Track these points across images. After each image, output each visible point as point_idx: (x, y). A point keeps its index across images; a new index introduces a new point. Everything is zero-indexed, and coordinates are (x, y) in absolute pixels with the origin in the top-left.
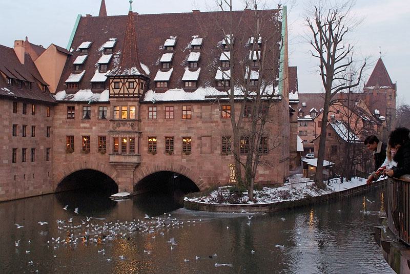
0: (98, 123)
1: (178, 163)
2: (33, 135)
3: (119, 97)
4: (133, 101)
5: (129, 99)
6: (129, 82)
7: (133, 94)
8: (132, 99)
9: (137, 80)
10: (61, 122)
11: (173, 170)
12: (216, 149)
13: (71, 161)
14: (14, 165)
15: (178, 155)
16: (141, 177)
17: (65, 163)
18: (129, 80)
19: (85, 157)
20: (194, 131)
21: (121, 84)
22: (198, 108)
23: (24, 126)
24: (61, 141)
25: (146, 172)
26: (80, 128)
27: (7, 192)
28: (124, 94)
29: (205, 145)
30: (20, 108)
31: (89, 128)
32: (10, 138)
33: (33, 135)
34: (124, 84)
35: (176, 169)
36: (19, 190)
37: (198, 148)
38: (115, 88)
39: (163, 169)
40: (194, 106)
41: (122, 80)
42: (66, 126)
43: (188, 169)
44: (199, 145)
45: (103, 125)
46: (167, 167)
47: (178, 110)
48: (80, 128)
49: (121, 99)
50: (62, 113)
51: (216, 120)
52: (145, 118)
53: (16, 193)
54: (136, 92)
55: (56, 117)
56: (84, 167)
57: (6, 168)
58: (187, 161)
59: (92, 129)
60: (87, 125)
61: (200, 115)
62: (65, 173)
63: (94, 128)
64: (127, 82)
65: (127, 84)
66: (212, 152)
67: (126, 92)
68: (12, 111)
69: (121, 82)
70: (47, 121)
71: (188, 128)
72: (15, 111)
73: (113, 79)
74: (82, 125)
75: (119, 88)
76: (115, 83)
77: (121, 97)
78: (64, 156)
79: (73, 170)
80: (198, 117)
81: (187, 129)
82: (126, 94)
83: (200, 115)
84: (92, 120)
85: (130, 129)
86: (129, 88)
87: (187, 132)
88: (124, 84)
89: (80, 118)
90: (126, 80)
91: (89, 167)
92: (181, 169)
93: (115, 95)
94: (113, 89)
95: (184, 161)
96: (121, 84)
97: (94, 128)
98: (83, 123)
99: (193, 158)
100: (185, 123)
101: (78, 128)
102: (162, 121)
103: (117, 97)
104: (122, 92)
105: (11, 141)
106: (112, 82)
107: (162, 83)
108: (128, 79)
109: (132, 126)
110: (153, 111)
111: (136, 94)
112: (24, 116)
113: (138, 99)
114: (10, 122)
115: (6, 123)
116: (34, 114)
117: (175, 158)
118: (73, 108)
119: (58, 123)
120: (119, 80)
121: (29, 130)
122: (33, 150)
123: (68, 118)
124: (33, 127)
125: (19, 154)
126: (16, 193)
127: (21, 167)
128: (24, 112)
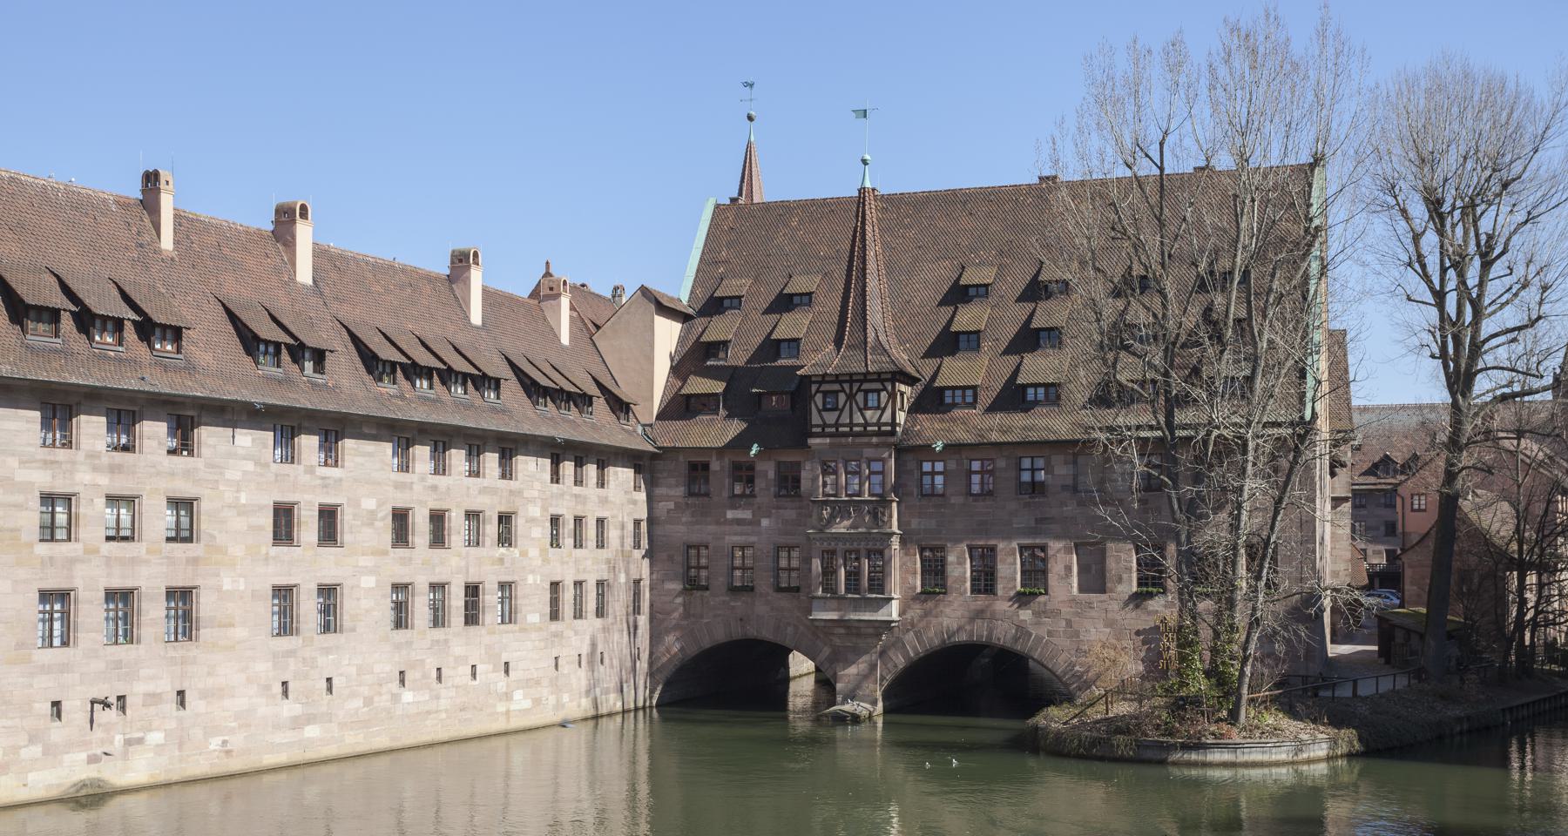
0: (778, 508)
2: (601, 544)
4: (877, 446)
5: (865, 440)
6: (866, 392)
7: (879, 424)
8: (874, 440)
10: (671, 505)
11: (994, 641)
14: (555, 626)
16: (901, 662)
18: (866, 386)
21: (842, 398)
22: (1066, 463)
23: (578, 520)
24: (671, 558)
25: (914, 648)
27: (537, 702)
28: (851, 425)
30: (568, 468)
32: (543, 551)
33: (601, 544)
34: (851, 397)
35: (1003, 634)
36: (566, 698)
38: (826, 409)
40: (1054, 458)
41: (846, 386)
43: (1039, 639)
45: (790, 514)
46: (979, 631)
49: (843, 440)
50: (672, 481)
53: (559, 706)
54: (887, 417)
56: (737, 633)
57: (534, 635)
59: (759, 523)
60: (746, 514)
61: (1069, 482)
63: (765, 522)
64: (859, 390)
67: (858, 419)
68: (548, 477)
69: (843, 390)
70: (635, 502)
71: (1039, 521)
72: (556, 477)
73: (821, 383)
74: (730, 514)
75: (835, 409)
76: (825, 394)
77: (845, 435)
78: (679, 600)
79: (707, 643)
80: (1065, 488)
81: (1032, 523)
83: (1069, 482)
84: (758, 500)
86: (867, 408)
87: (1033, 532)
88: (851, 397)
89: (725, 494)
91: (752, 632)
92: (1016, 639)
94: (819, 411)
95: (1026, 615)
96: (842, 398)
97: (765, 522)
98: (734, 507)
101: (718, 523)
102: (956, 500)
103: (831, 435)
105: (546, 561)
107: (958, 393)
108: (862, 382)
110: (933, 473)
111: (886, 424)
112: (577, 490)
113: (892, 440)
114: (544, 509)
115: (535, 511)
116: (601, 483)
118: (706, 466)
119: (663, 507)
120: (836, 387)
121: (591, 531)
122: (600, 584)
123: (691, 494)
124: (601, 522)
125: (568, 596)
126: (559, 706)
127: (571, 633)
128: (578, 481)
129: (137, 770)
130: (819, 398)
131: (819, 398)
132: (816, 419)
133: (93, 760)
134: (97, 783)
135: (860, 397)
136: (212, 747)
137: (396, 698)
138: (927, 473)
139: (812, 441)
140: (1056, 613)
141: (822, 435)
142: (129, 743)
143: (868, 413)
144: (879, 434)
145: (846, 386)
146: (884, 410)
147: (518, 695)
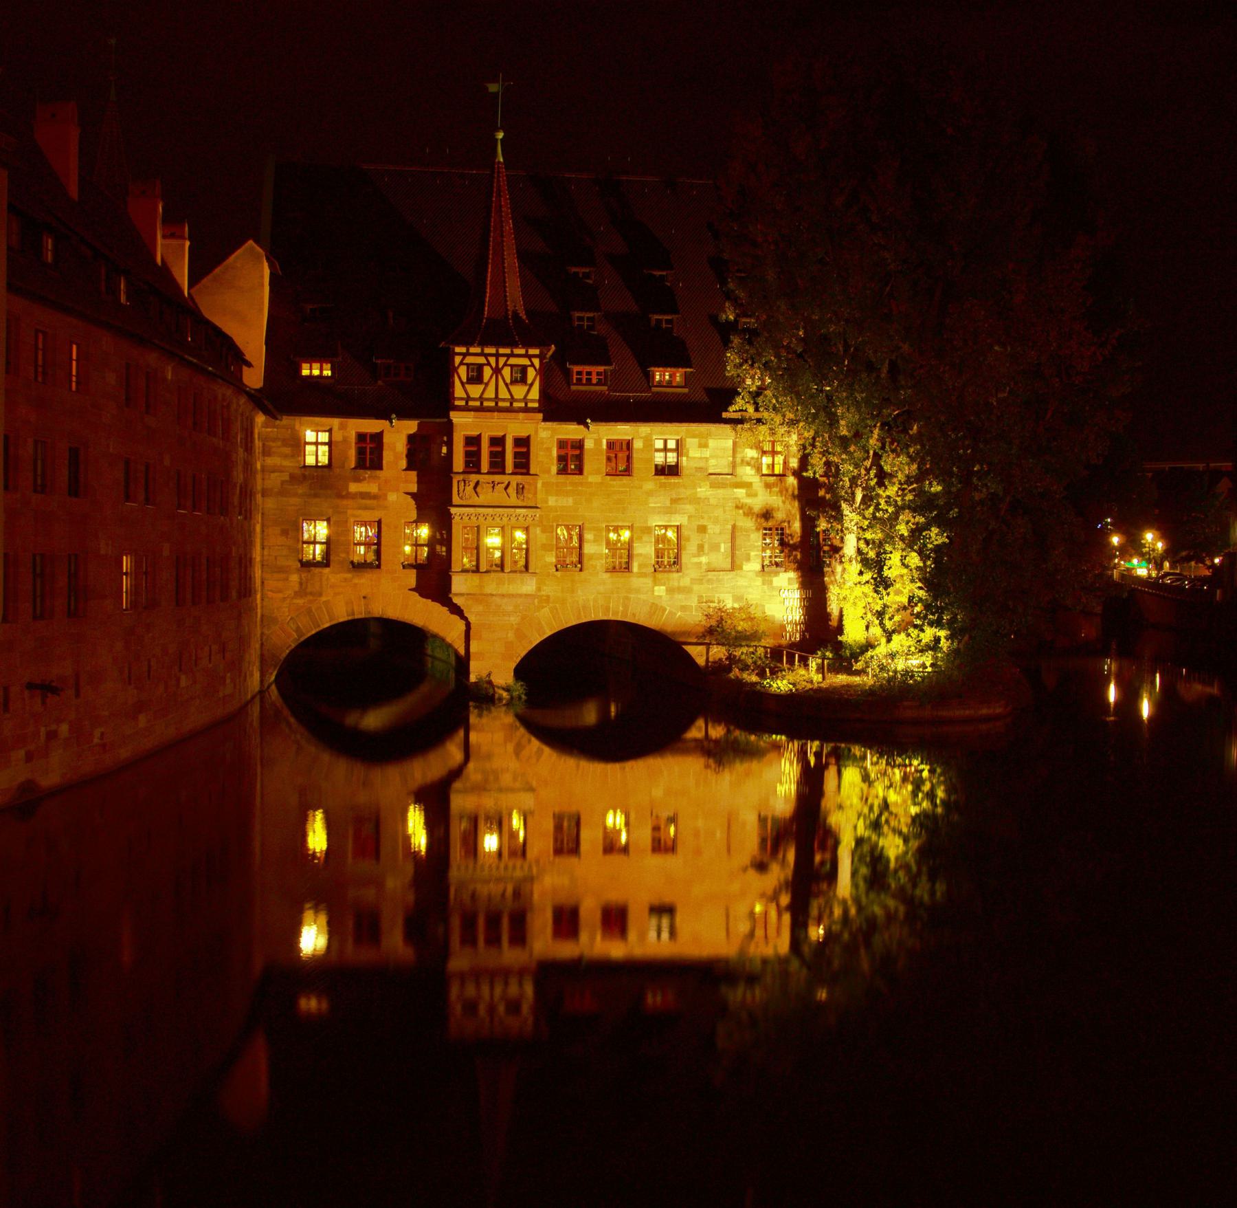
1: (642, 597)
3: (481, 409)
7: (525, 400)
8: (521, 415)
9: (536, 362)
10: (286, 477)
12: (748, 559)
13: (320, 595)
15: (644, 575)
16: (537, 639)
17: (300, 601)
18: (512, 361)
19: (363, 581)
20: (690, 508)
21: (487, 372)
26: (350, 496)
29: (715, 547)
31: (375, 497)
34: (497, 371)
37: (699, 556)
39: (601, 616)
41: (492, 360)
42: (301, 490)
44: (701, 548)
47: (642, 450)
48: (350, 496)
51: (746, 479)
52: (548, 471)
54: (535, 394)
55: (270, 461)
58: (670, 591)
62: (298, 630)
64: (505, 364)
65: (506, 372)
66: (734, 566)
67: (504, 393)
71: (674, 501)
74: (354, 487)
77: (489, 410)
78: (294, 578)
81: (668, 503)
82: (504, 400)
83: (702, 464)
85: (514, 500)
87: (669, 511)
88: (497, 371)
90: (502, 361)
93: (471, 403)
95: (660, 590)
97: (392, 497)
98: (358, 480)
99: (685, 581)
100: (662, 486)
104: (490, 393)
106: (461, 363)
108: (508, 356)
109: (520, 490)
111: (533, 401)
117: (636, 582)
129: (52, 774)
130: (463, 371)
131: (463, 371)
132: (459, 392)
133: (29, 757)
134: (28, 787)
135: (506, 372)
136: (96, 741)
137: (178, 680)
138: (671, 450)
139: (453, 414)
140: (686, 590)
141: (466, 409)
142: (52, 735)
143: (512, 388)
144: (526, 410)
145: (492, 360)
146: (531, 385)
147: (228, 681)
